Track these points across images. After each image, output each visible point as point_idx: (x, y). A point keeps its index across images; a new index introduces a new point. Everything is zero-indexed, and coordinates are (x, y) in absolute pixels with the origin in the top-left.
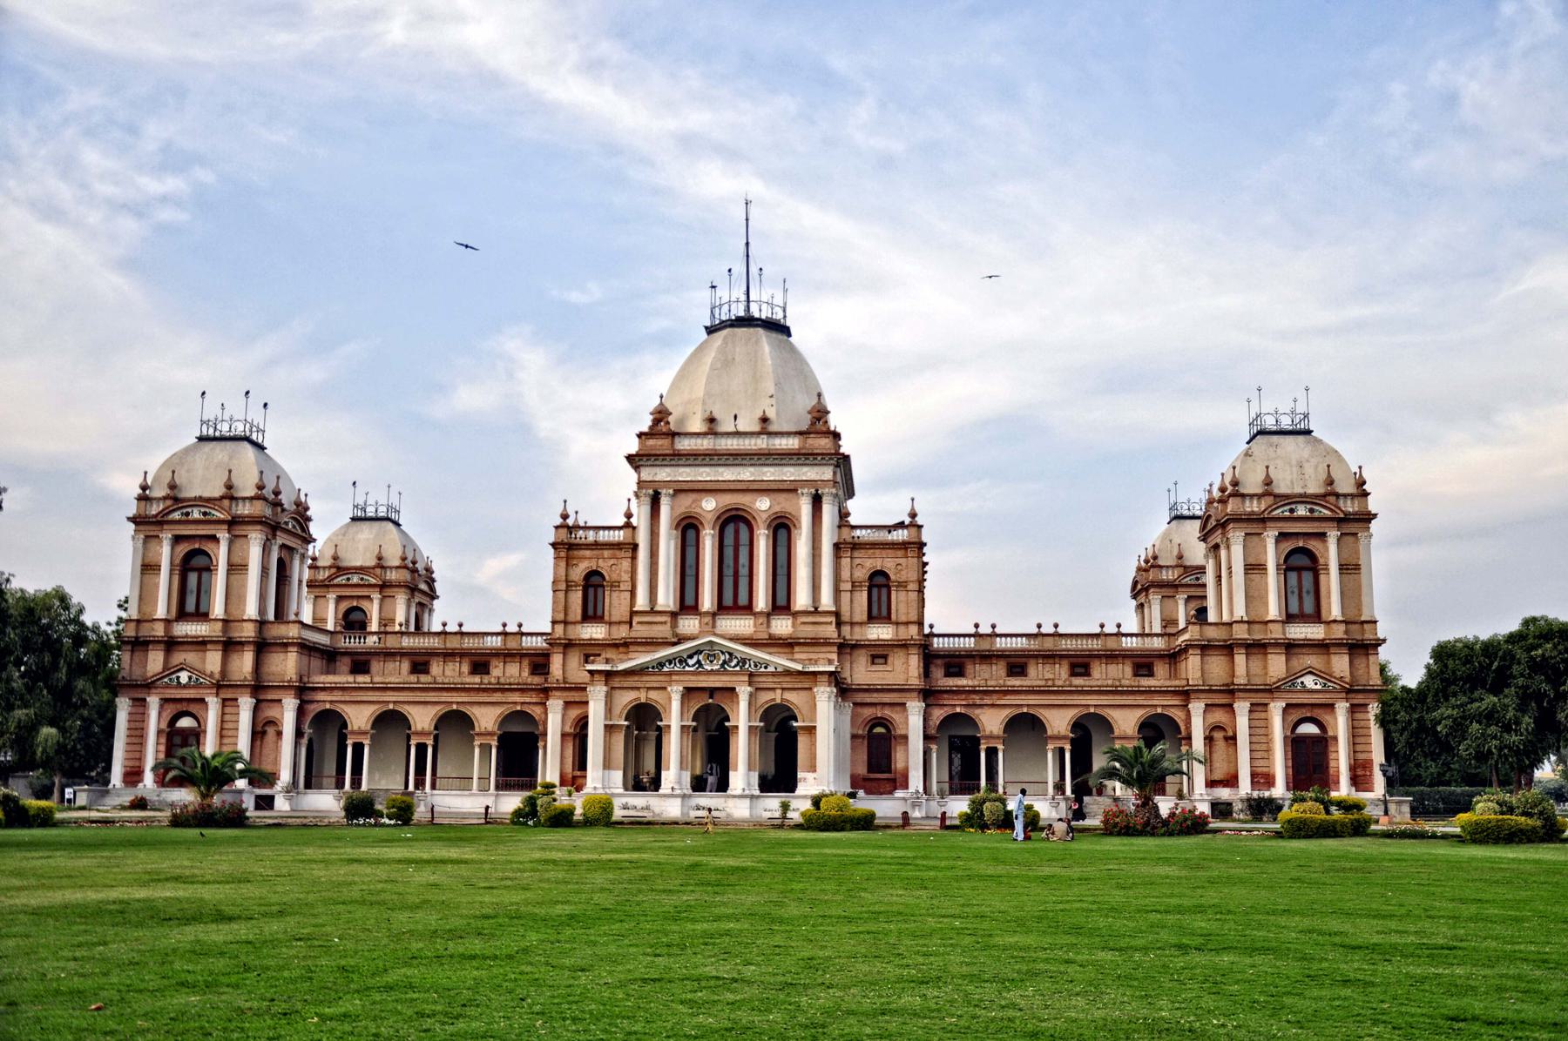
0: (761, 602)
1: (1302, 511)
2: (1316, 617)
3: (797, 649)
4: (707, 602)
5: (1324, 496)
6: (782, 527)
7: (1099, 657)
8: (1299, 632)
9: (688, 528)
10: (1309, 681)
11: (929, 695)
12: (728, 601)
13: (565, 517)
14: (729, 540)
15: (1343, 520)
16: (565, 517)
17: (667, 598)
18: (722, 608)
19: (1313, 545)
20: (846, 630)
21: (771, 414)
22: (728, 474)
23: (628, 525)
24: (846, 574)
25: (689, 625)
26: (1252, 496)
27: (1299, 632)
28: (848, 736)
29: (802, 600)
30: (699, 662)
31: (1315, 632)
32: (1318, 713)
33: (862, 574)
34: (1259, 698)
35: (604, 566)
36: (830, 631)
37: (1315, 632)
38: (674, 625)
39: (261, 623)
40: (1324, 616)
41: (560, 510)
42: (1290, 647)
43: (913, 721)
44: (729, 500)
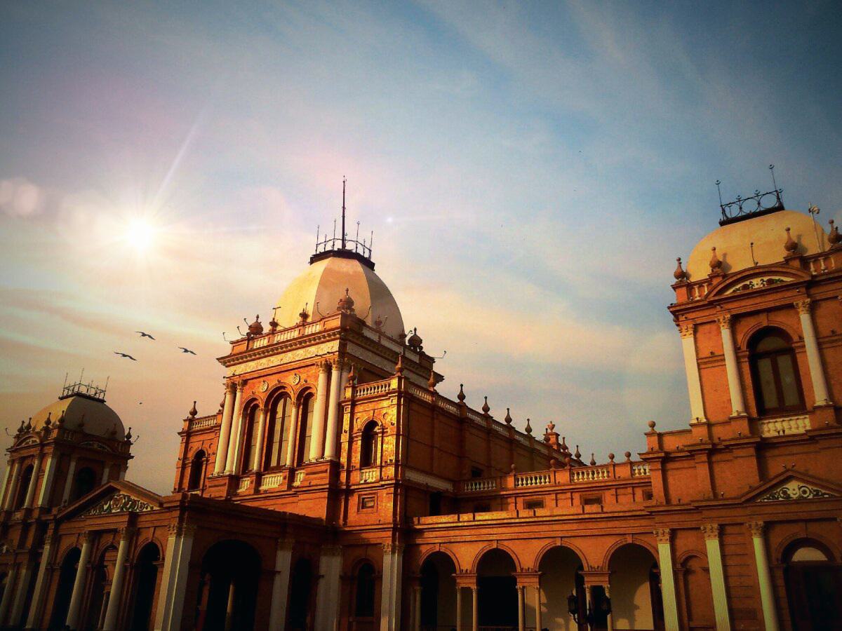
0: (288, 460)
1: (757, 283)
2: (800, 407)
3: (302, 497)
4: (255, 466)
5: (787, 260)
6: (305, 398)
7: (608, 488)
8: (771, 428)
9: (250, 410)
10: (793, 489)
11: (405, 533)
12: (274, 463)
13: (194, 412)
14: (279, 415)
15: (812, 283)
16: (194, 412)
17: (231, 467)
18: (267, 468)
19: (780, 320)
20: (343, 476)
21: (310, 311)
22: (275, 360)
23: (221, 412)
24: (346, 426)
25: (246, 485)
26: (700, 284)
27: (771, 428)
28: (338, 577)
29: (312, 453)
30: (110, 505)
31: (798, 425)
32: (815, 530)
33: (359, 424)
34: (727, 515)
35: (206, 445)
36: (323, 480)
37: (798, 425)
38: (237, 487)
39: (45, 510)
40: (809, 406)
41: (190, 408)
42: (763, 447)
43: (391, 564)
44: (273, 382)
